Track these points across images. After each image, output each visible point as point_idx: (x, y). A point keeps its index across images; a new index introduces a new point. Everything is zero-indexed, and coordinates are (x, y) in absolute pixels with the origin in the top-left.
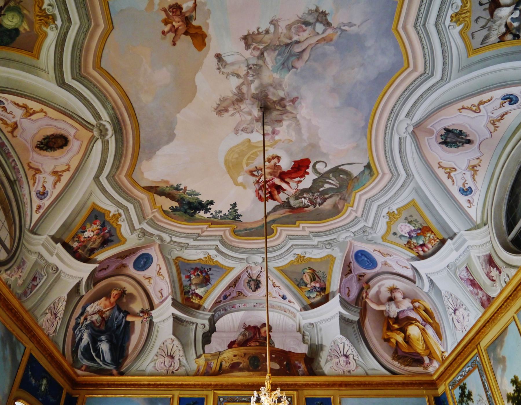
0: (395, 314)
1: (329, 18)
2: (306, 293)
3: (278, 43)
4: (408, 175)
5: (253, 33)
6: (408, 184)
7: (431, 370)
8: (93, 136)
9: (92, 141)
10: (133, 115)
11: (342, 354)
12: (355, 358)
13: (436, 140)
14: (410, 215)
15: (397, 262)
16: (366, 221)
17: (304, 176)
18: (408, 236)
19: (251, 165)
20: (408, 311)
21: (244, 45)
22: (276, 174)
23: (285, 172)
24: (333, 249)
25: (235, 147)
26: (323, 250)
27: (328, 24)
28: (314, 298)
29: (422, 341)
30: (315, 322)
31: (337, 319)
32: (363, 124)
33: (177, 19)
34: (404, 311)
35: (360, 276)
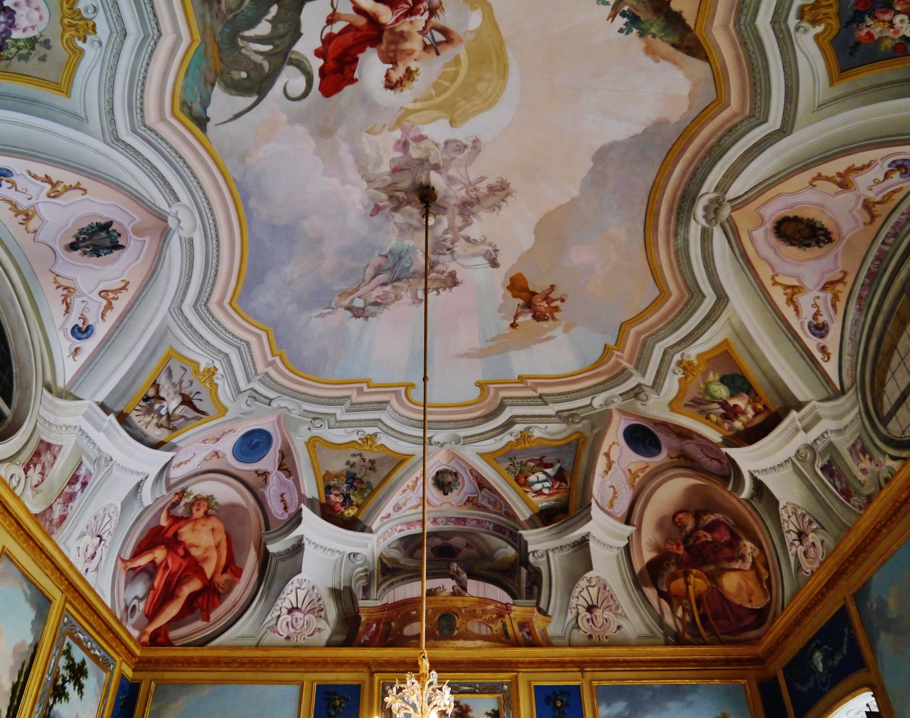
1: (349, 313)
3: (411, 280)
4: (118, 139)
5: (445, 289)
8: (734, 209)
9: (739, 203)
10: (651, 215)
14: (47, 59)
17: (323, 41)
19: (448, 60)
21: (457, 276)
22: (391, 37)
23: (371, 46)
25: (481, 111)
27: (348, 308)
32: (252, 203)
33: (542, 309)
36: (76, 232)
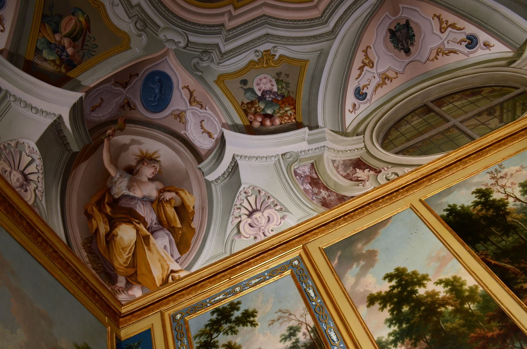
0: (118, 193)
2: (42, 40)
6: (322, 40)
7: (122, 297)
11: (21, 168)
12: (37, 191)
13: (390, 25)
15: (203, 121)
16: (227, 40)
18: (260, 95)
20: (139, 202)
24: (140, 36)
26: (130, 21)
28: (46, 60)
29: (130, 253)
30: (7, 91)
31: (49, 121)
34: (133, 198)
35: (128, 104)
36: (396, 50)
